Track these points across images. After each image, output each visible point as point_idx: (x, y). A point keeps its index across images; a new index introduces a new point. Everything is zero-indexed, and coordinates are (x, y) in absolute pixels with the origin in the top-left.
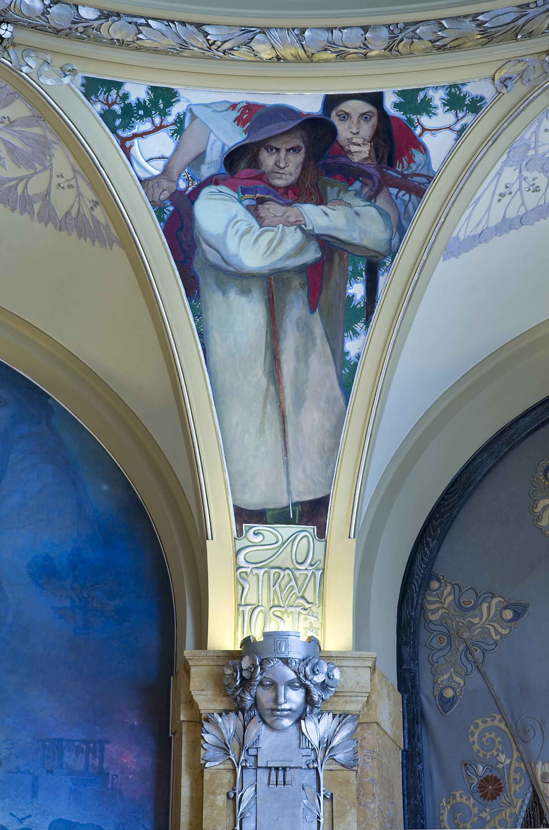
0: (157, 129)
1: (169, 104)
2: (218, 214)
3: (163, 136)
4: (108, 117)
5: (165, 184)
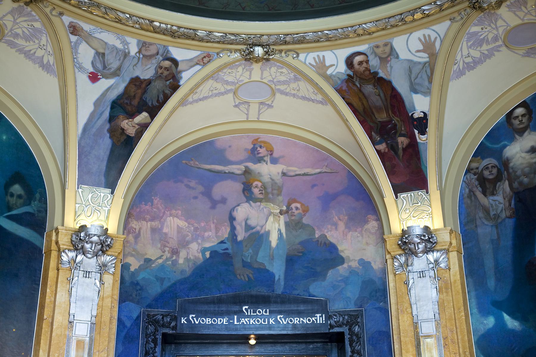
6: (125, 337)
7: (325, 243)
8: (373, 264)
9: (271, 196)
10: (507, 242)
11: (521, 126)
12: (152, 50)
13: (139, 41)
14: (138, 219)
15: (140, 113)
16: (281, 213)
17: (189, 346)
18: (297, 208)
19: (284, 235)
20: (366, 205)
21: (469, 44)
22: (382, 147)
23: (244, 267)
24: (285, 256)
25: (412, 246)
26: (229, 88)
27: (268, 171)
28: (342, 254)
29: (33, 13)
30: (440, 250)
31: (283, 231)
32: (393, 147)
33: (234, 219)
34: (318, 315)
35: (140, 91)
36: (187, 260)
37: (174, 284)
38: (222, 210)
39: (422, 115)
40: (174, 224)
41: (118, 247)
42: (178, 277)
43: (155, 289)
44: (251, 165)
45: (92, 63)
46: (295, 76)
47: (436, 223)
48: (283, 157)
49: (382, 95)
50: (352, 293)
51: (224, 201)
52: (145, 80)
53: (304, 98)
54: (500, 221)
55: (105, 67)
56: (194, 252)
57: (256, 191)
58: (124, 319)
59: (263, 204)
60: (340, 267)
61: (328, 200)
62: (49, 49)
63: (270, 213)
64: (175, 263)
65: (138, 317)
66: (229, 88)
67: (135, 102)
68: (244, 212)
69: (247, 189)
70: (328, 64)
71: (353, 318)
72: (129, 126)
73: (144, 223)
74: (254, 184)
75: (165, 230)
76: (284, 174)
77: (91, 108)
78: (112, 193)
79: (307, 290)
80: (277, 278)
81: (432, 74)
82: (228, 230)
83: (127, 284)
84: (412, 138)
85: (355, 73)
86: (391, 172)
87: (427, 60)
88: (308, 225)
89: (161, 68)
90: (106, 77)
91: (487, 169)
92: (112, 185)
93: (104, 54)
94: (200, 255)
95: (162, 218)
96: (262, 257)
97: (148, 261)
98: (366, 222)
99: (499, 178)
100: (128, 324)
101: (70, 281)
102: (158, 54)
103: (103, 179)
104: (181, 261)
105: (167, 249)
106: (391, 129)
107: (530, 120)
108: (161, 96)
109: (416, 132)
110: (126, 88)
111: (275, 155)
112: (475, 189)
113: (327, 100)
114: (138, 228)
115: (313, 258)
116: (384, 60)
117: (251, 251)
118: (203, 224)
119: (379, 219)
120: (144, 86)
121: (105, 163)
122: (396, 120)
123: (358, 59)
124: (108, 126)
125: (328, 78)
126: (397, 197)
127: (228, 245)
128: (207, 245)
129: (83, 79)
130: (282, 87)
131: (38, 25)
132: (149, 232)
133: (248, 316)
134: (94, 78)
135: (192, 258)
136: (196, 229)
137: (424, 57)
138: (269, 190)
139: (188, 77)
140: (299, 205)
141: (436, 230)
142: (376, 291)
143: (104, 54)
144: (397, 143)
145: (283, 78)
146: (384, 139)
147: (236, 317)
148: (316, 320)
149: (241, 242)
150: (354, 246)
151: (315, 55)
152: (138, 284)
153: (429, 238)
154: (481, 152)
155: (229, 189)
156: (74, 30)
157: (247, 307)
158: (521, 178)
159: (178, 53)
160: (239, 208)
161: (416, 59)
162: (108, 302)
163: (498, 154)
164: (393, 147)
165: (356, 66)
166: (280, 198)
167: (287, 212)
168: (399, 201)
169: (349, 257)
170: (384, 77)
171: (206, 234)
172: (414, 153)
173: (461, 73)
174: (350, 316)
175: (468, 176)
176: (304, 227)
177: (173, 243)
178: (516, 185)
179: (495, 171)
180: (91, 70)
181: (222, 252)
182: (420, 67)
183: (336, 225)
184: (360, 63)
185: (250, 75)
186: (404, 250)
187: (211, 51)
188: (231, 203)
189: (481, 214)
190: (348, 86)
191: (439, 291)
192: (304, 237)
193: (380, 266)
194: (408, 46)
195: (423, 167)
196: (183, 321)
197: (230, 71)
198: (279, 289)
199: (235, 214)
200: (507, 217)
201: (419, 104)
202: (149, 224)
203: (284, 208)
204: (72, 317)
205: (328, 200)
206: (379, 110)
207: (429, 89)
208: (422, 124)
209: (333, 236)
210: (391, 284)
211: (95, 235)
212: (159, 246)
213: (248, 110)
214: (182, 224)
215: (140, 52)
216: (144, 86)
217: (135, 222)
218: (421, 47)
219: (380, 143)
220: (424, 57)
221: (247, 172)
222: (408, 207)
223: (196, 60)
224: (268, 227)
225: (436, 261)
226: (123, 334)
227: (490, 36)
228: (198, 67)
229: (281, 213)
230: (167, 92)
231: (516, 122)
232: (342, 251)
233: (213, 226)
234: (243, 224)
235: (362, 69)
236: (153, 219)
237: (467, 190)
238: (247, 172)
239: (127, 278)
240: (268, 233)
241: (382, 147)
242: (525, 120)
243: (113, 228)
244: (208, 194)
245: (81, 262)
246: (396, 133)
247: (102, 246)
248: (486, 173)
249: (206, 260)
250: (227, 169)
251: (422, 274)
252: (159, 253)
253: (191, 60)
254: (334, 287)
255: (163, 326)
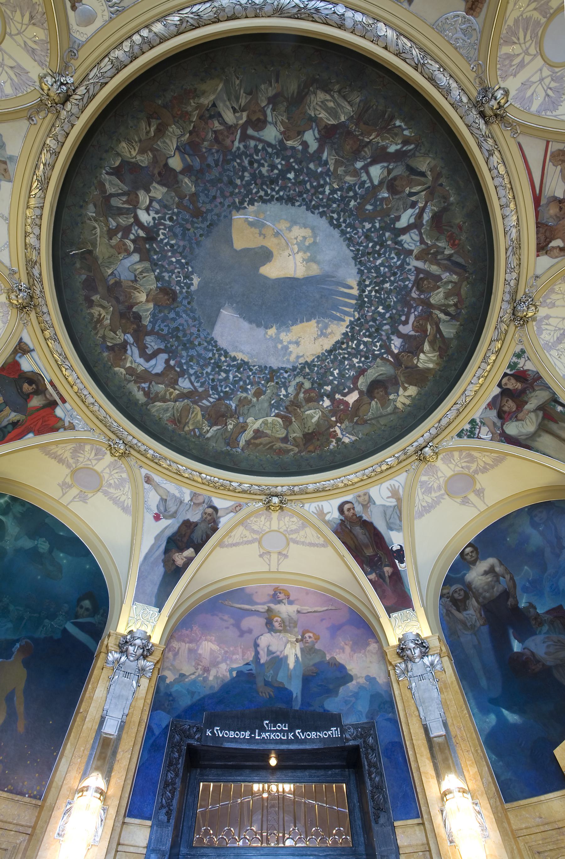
0: (480, 428)
1: (475, 422)
2: (512, 429)
3: (482, 428)
4: (469, 437)
5: (495, 436)
6: (152, 745)
7: (335, 664)
8: (378, 679)
9: (288, 628)
10: (487, 644)
11: (473, 559)
12: (200, 499)
13: (191, 492)
14: (179, 640)
15: (188, 548)
16: (297, 641)
17: (214, 771)
18: (310, 637)
19: (300, 659)
20: (365, 630)
21: (423, 490)
22: (373, 576)
23: (265, 685)
24: (301, 677)
25: (409, 652)
26: (255, 536)
27: (285, 610)
28: (350, 673)
29: (123, 466)
30: (434, 655)
31: (299, 655)
32: (381, 576)
33: (258, 646)
34: (333, 729)
35: (189, 531)
36: (216, 677)
37: (203, 698)
38: (249, 638)
39: (399, 547)
40: (208, 647)
41: (157, 656)
42: (207, 692)
43: (185, 702)
44: (272, 606)
45: (157, 506)
46: (302, 523)
47: (425, 631)
48: (297, 600)
49: (367, 534)
50: (363, 707)
51: (250, 631)
52: (193, 522)
53: (311, 545)
54: (476, 629)
55: (166, 510)
56: (223, 671)
57: (276, 625)
58: (154, 727)
59: (282, 635)
60: (349, 684)
61: (335, 630)
62: (130, 496)
63: (288, 641)
64: (205, 679)
65: (167, 726)
66: (255, 536)
67: (185, 540)
68: (267, 640)
69: (269, 624)
70: (325, 512)
71: (367, 730)
72: (179, 559)
73: (183, 644)
74: (275, 619)
75: (200, 651)
76: (298, 612)
77: (152, 541)
78: (160, 612)
79: (322, 706)
80: (294, 695)
81: (401, 514)
82: (253, 654)
83: (162, 694)
84: (395, 566)
85: (346, 517)
86: (382, 597)
87: (396, 503)
88: (320, 650)
89: (206, 513)
90: (165, 518)
91: (454, 594)
92: (160, 605)
93: (166, 500)
94: (228, 674)
95: (198, 641)
96: (281, 677)
97: (182, 676)
98: (368, 645)
99: (466, 597)
100: (157, 732)
101: (110, 679)
102: (204, 502)
103: (154, 600)
104: (211, 678)
105: (200, 667)
106: (378, 561)
107: (477, 553)
108: (204, 536)
109: (397, 561)
110: (180, 528)
111: (291, 598)
112: (450, 609)
113: (328, 543)
114: (177, 647)
115: (325, 677)
116: (365, 507)
117: (271, 672)
118: (232, 649)
119: (378, 641)
120: (192, 527)
121: (157, 587)
122: (380, 553)
123: (346, 507)
124: (163, 557)
125: (327, 523)
126: (390, 617)
127: (252, 666)
128: (235, 666)
129: (149, 517)
130: (294, 536)
131: (124, 475)
132: (186, 652)
133: (268, 731)
134: (157, 518)
135: (221, 676)
136: (226, 652)
137: (393, 502)
138: (287, 624)
139: (224, 522)
140: (311, 635)
141: (427, 638)
142: (384, 703)
143: (166, 500)
144: (384, 572)
145: (294, 527)
146: (373, 571)
147: (257, 731)
148: (332, 734)
149: (263, 664)
150: (361, 666)
151: (315, 504)
152: (171, 695)
153: (423, 646)
154: (448, 581)
155: (255, 623)
156: (148, 480)
157: (267, 722)
158: (484, 594)
159: (218, 503)
160: (262, 637)
161: (388, 504)
162: (140, 703)
163: (462, 580)
164: (381, 576)
165: (346, 512)
166: (296, 630)
167: (302, 640)
168: (392, 619)
169: (356, 675)
170: (367, 519)
171: (234, 657)
172: (397, 578)
173: (421, 515)
174: (363, 728)
175: (443, 599)
176: (316, 651)
177: (206, 663)
178: (481, 600)
179: (462, 593)
180: (156, 511)
181: (247, 672)
182: (392, 509)
183: (343, 649)
184: (349, 510)
185: (270, 525)
186: (402, 657)
187: (243, 501)
188: (256, 633)
189: (460, 627)
190: (342, 528)
191: (440, 691)
192: (317, 660)
193: (385, 680)
194: (381, 494)
195: (406, 590)
196: (209, 733)
197: (255, 519)
198: (297, 706)
199: (259, 641)
200: (481, 625)
201: (396, 540)
202: (187, 645)
203: (300, 637)
204: (105, 712)
205: (335, 630)
206: (367, 546)
207: (400, 526)
208: (400, 555)
209: (341, 658)
210: (397, 692)
211: (139, 638)
212: (194, 664)
213: (270, 561)
214: (215, 647)
215: (191, 500)
216: (192, 527)
217: (176, 643)
218: (390, 495)
219: (370, 573)
220: (393, 502)
221: (269, 610)
222: (400, 624)
223: (231, 509)
224: (286, 652)
225: (432, 664)
226: (151, 741)
227: (435, 485)
228: (232, 514)
229: (297, 641)
230: (209, 533)
231: (468, 557)
232: (350, 670)
233: (240, 650)
234: (266, 650)
235: (350, 514)
236: (191, 642)
237: (445, 611)
238: (269, 610)
239: (162, 688)
240: (286, 657)
241: (373, 576)
242: (474, 554)
243: (156, 639)
244: (237, 625)
245: (124, 663)
246: (381, 564)
247: (144, 651)
248: (456, 595)
249: (233, 679)
250: (253, 608)
251: (421, 677)
252: (193, 670)
253: (227, 508)
254: (346, 702)
255: (189, 737)
